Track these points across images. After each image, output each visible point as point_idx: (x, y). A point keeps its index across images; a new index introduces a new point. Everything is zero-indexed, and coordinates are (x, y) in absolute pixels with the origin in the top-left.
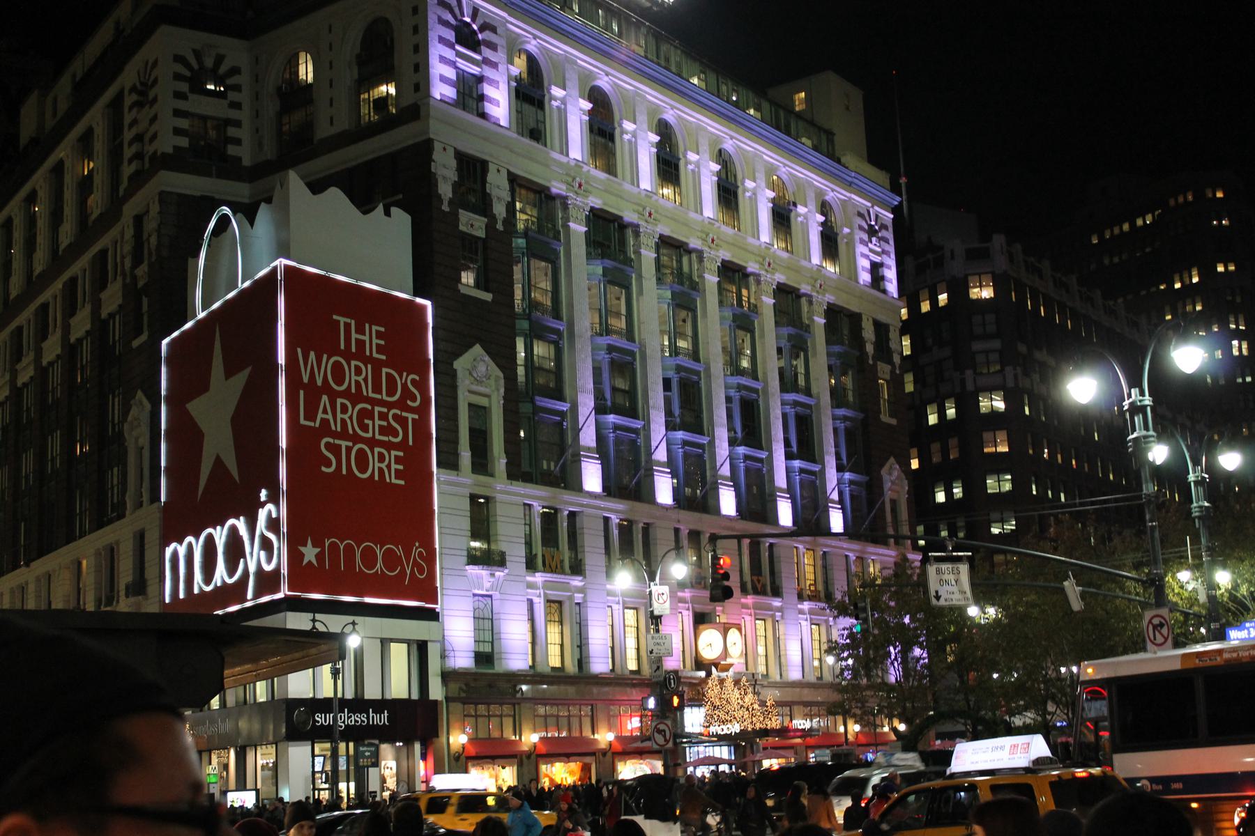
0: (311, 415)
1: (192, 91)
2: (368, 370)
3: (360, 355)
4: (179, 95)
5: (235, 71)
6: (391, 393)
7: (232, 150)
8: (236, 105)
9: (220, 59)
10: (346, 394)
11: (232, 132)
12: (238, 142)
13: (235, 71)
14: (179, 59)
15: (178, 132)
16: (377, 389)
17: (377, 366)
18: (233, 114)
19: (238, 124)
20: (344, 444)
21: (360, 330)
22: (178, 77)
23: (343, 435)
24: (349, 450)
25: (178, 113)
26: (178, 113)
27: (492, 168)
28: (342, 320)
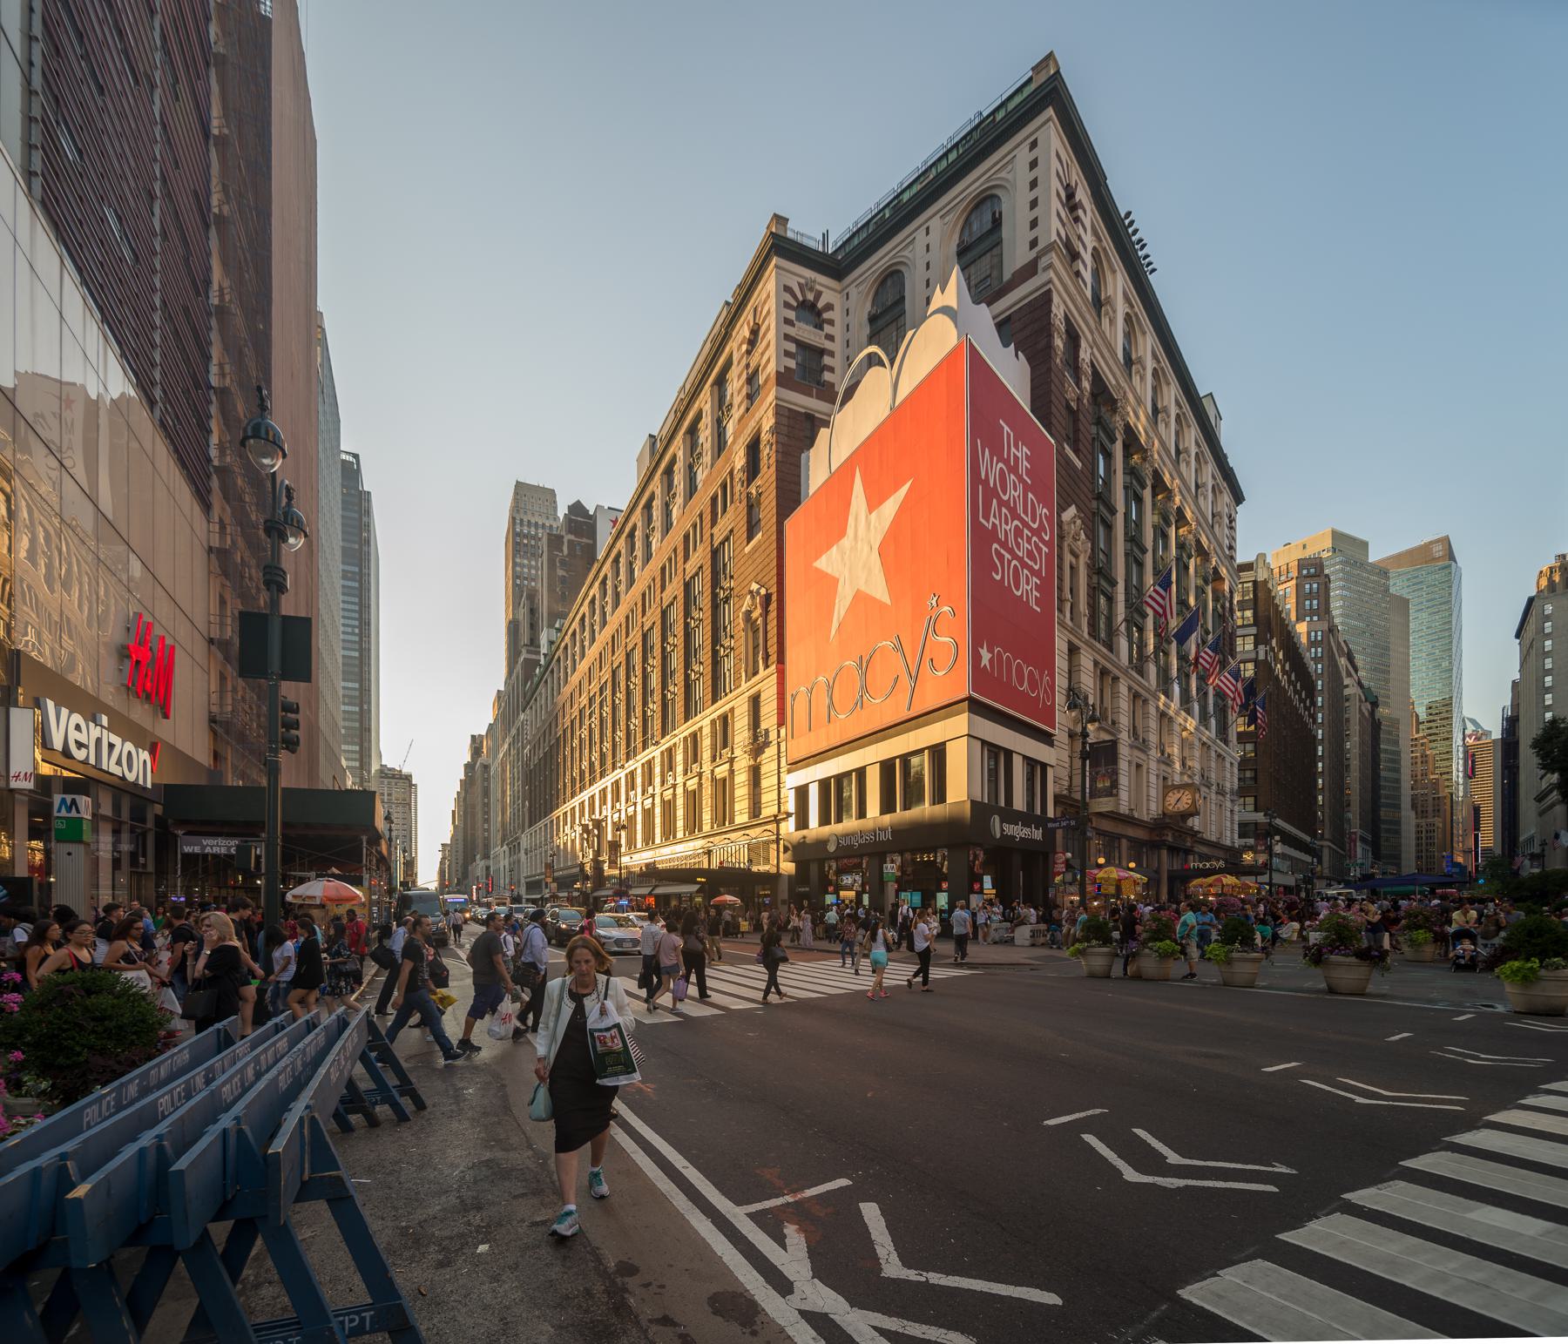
0: (987, 519)
1: (798, 318)
2: (1020, 488)
3: (1014, 470)
4: (788, 322)
5: (829, 307)
6: (1034, 521)
7: (827, 376)
8: (830, 338)
9: (818, 295)
10: (1005, 504)
11: (827, 360)
12: (832, 370)
13: (829, 307)
14: (787, 289)
15: (787, 354)
16: (1026, 512)
17: (1026, 489)
18: (828, 345)
19: (832, 354)
20: (1007, 556)
21: (1017, 447)
22: (787, 305)
23: (1004, 545)
24: (1009, 562)
25: (787, 337)
26: (787, 337)
27: (1083, 344)
28: (1006, 428)
